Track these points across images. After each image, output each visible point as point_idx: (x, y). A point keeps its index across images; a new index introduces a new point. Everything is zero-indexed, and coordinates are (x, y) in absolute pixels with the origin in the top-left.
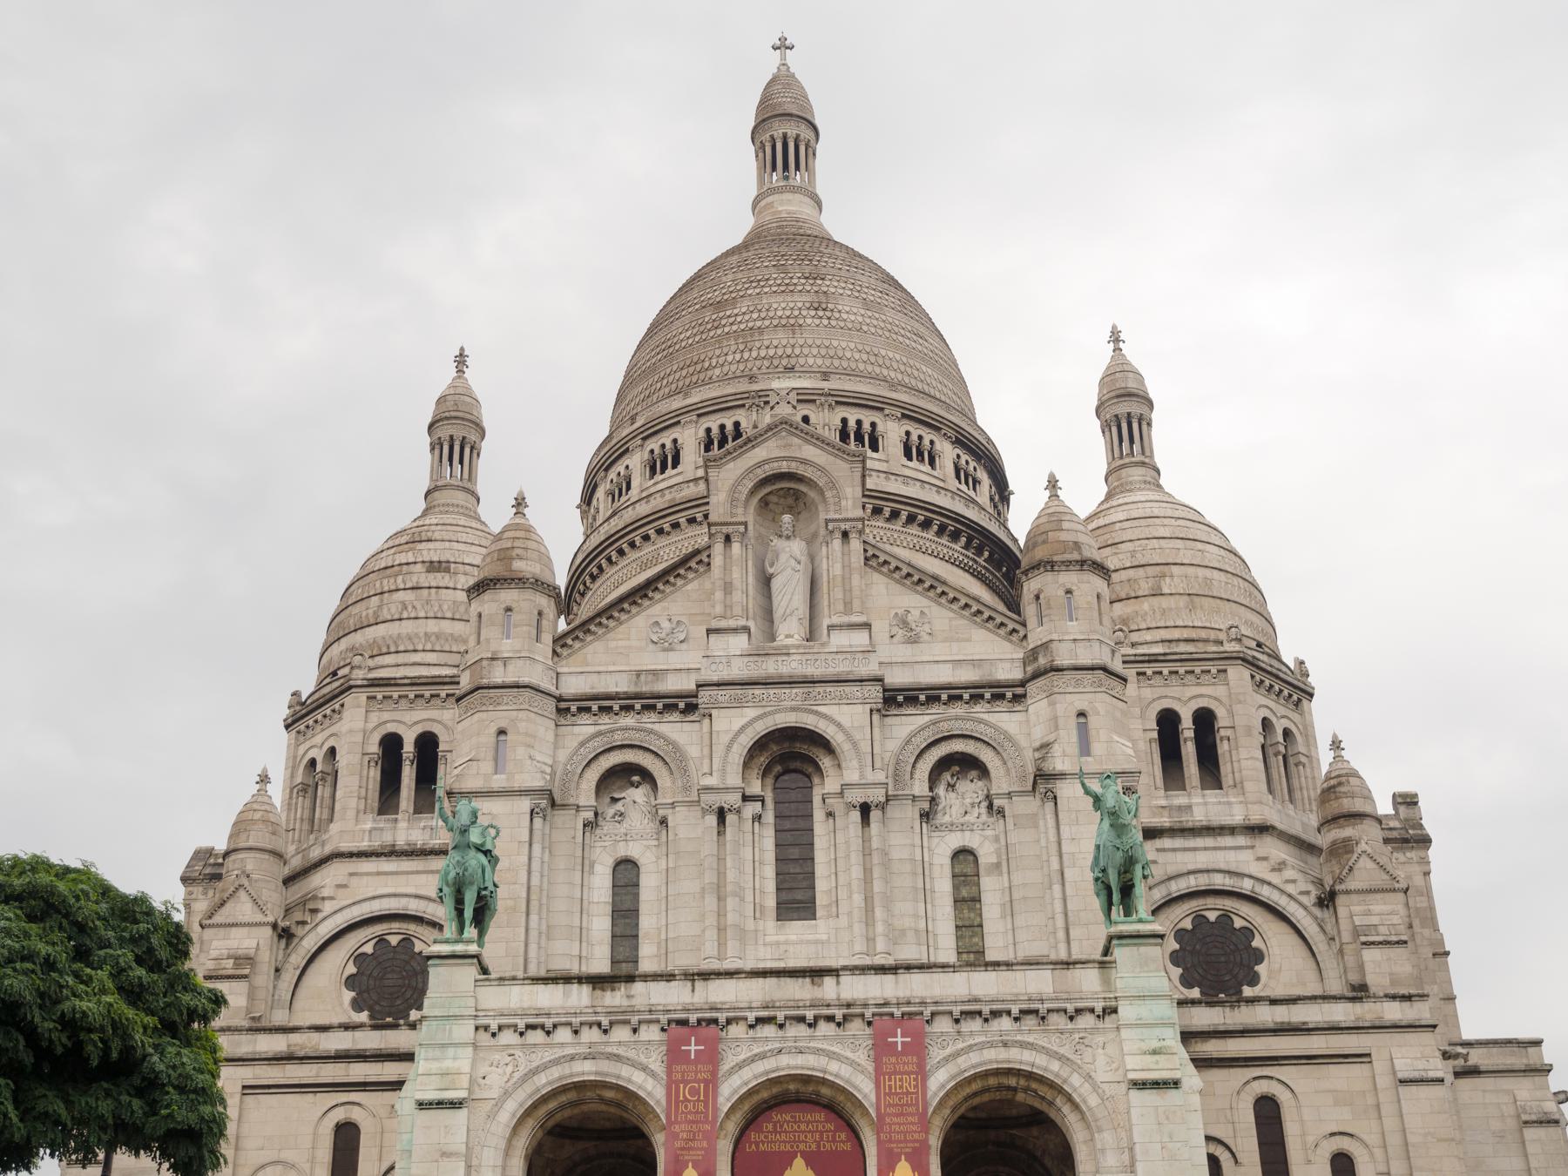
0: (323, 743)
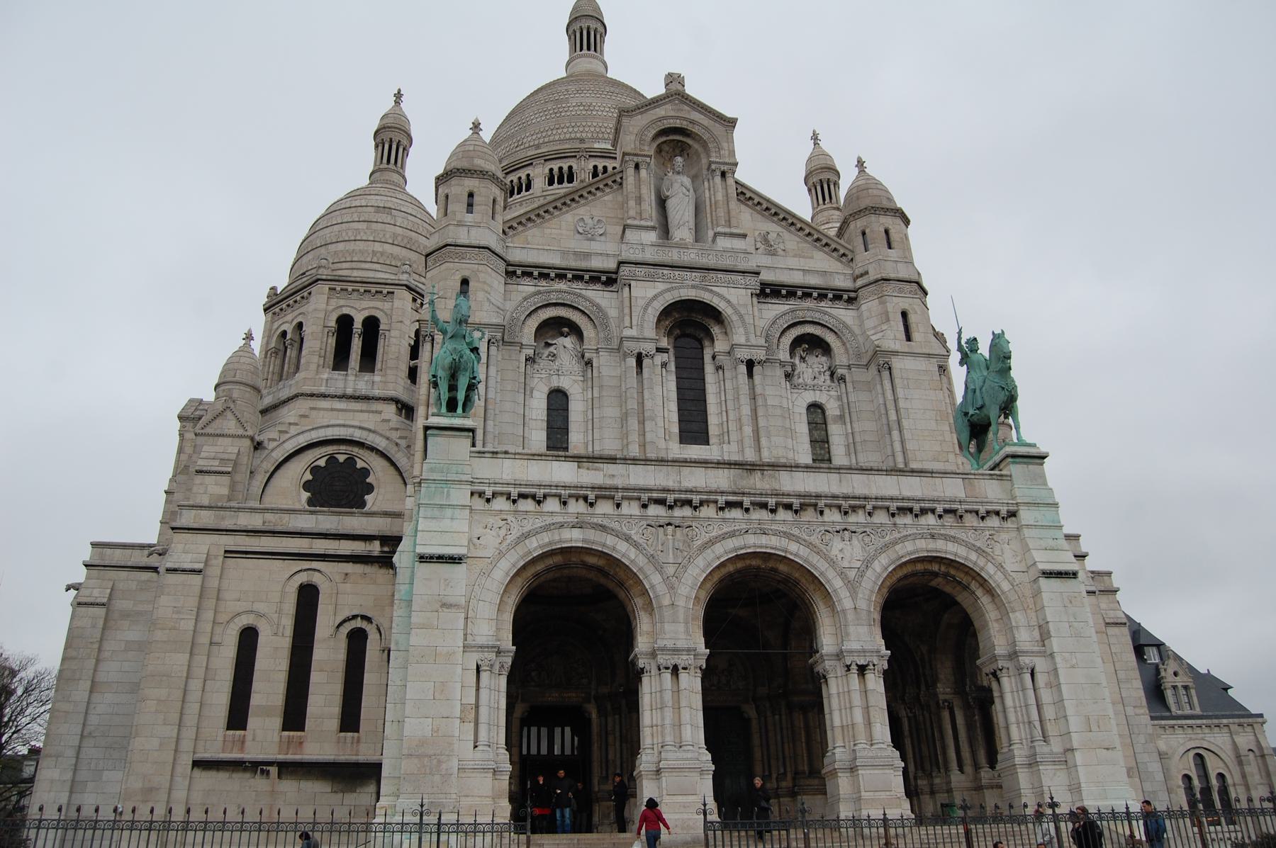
0: (293, 320)
